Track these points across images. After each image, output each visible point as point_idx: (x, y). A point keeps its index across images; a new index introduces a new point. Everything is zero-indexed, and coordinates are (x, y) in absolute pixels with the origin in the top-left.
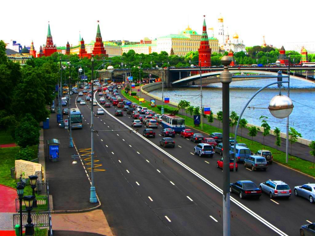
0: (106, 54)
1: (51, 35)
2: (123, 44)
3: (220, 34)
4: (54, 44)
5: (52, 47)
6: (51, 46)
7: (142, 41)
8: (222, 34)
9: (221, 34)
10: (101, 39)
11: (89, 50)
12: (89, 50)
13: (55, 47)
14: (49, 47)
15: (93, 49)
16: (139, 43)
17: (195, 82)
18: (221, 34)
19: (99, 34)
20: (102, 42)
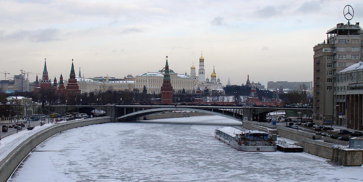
0: (79, 90)
1: (47, 71)
2: (107, 80)
3: (201, 73)
4: (49, 79)
5: (47, 82)
6: (46, 81)
7: (125, 78)
8: (203, 73)
9: (202, 73)
10: (75, 76)
11: (65, 85)
12: (65, 85)
13: (50, 82)
14: (45, 82)
15: (67, 85)
16: (123, 80)
17: (147, 116)
18: (202, 73)
19: (73, 71)
20: (76, 78)
